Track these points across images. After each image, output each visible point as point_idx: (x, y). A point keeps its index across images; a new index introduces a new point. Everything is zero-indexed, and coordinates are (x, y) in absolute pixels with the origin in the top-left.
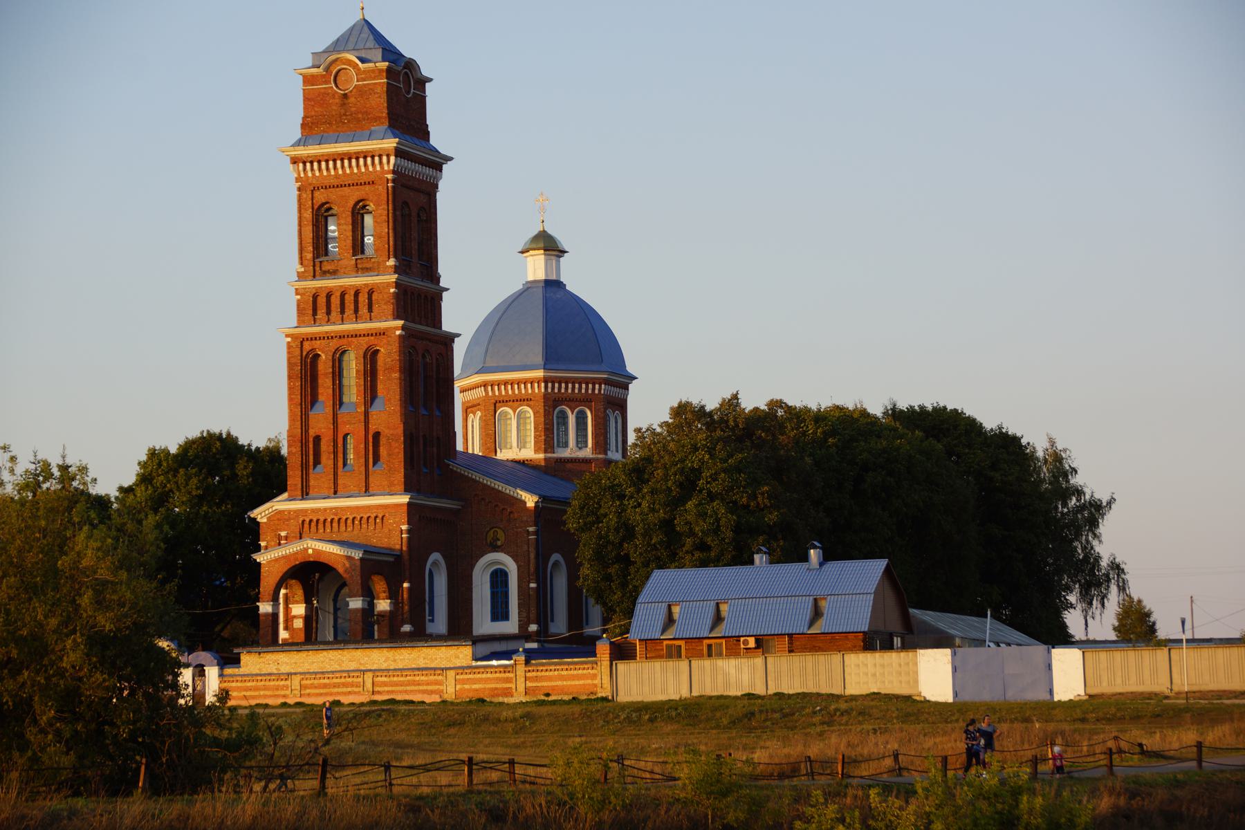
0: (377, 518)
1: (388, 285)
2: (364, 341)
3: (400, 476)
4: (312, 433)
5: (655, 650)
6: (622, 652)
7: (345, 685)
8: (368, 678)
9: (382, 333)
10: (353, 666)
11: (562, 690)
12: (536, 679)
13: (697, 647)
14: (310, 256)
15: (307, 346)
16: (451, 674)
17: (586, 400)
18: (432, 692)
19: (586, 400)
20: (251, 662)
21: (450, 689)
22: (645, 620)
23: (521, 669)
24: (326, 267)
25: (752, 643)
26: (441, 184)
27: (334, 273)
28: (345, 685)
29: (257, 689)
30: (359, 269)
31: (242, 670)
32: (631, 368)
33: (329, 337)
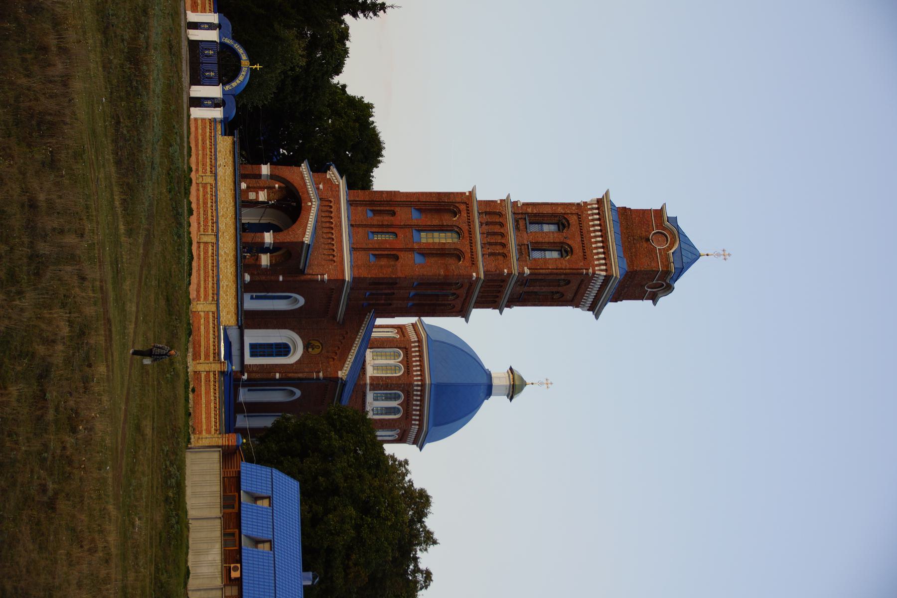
0: (334, 256)
1: (509, 268)
2: (466, 249)
3: (364, 273)
4: (397, 209)
5: (231, 486)
6: (228, 455)
7: (206, 219)
8: (211, 239)
9: (474, 263)
10: (222, 226)
11: (197, 403)
12: (208, 381)
13: (232, 521)
14: (529, 210)
15: (463, 207)
16: (214, 308)
17: (407, 415)
18: (198, 292)
19: (407, 415)
20: (225, 144)
21: (201, 307)
22: (255, 476)
23: (216, 367)
24: (521, 223)
25: (235, 574)
26: (578, 310)
27: (517, 228)
28: (206, 219)
29: (204, 148)
30: (521, 247)
31: (220, 138)
32: (428, 446)
33: (470, 223)
